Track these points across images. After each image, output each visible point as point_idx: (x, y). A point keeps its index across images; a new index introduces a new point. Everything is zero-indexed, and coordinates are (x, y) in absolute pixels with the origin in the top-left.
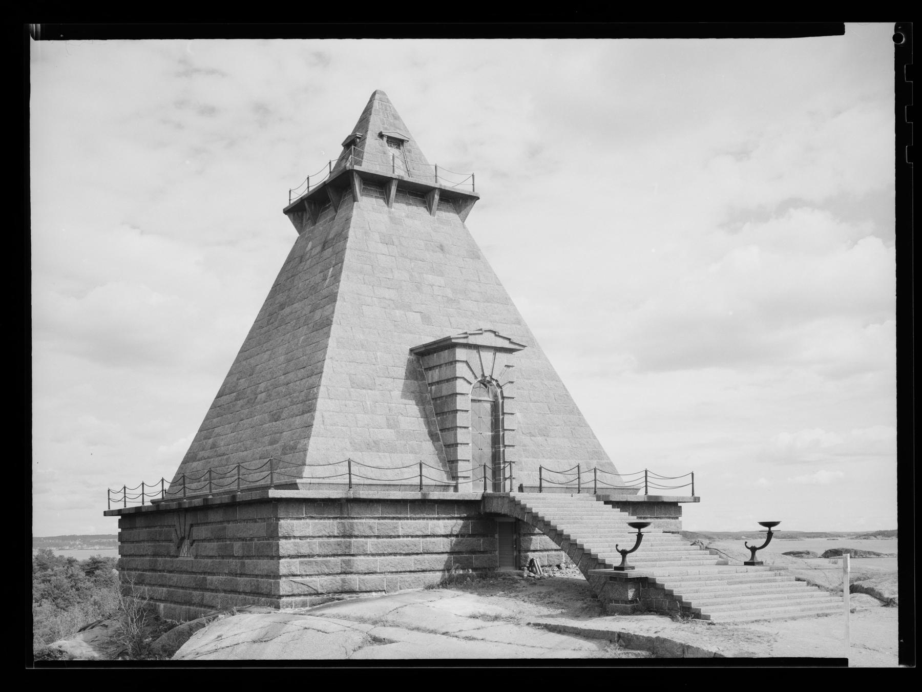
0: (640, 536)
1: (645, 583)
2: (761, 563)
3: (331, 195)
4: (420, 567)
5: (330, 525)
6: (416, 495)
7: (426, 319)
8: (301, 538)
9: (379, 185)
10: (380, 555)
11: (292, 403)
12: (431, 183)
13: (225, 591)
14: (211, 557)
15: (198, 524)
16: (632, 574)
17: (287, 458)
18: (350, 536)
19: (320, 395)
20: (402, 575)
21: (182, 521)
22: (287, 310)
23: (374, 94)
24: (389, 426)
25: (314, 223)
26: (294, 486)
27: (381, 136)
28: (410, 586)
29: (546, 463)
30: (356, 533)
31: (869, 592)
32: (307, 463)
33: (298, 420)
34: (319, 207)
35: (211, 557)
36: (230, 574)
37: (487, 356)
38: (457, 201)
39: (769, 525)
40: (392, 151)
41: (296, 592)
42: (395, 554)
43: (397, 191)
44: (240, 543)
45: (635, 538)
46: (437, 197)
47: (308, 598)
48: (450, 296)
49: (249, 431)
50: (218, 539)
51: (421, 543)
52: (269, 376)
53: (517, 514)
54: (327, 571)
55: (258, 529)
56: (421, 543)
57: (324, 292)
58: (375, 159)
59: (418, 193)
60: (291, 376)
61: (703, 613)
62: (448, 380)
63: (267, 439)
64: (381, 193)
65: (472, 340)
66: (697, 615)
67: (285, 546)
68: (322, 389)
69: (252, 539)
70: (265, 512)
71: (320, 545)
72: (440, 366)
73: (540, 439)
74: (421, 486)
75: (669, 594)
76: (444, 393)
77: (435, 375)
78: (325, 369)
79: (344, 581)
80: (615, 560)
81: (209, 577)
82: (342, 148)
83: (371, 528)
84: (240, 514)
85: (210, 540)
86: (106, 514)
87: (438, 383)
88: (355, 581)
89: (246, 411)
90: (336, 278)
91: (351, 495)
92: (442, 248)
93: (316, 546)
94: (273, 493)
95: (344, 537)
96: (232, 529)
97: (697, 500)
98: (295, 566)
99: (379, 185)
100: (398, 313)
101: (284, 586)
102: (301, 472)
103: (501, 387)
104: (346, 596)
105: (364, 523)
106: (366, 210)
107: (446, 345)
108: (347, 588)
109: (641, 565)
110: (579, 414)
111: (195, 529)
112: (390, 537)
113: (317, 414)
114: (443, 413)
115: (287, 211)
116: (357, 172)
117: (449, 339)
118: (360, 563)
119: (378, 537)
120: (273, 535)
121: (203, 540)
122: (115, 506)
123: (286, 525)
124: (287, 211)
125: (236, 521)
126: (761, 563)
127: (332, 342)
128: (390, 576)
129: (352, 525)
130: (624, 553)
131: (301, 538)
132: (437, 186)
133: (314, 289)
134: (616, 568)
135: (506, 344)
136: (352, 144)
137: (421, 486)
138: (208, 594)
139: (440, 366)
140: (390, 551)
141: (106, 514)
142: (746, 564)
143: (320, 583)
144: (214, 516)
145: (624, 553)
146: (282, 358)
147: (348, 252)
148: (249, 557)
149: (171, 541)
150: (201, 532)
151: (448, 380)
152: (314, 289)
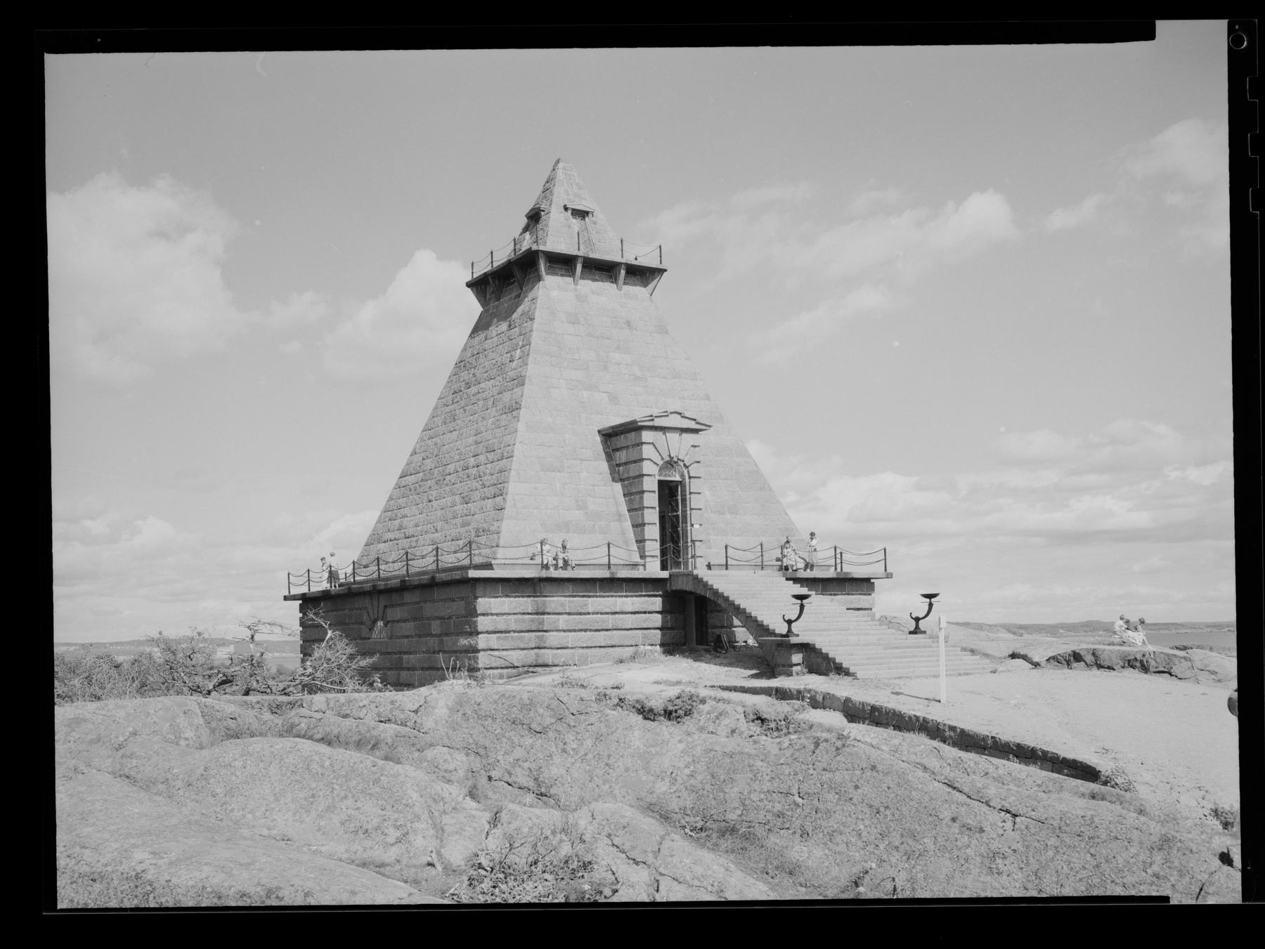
0: (802, 607)
1: (806, 648)
2: (925, 632)
3: (517, 273)
4: (609, 643)
5: (524, 603)
6: (605, 574)
7: (614, 399)
8: (497, 615)
9: (563, 263)
10: (570, 631)
11: (484, 486)
12: (618, 259)
13: (423, 669)
14: (407, 637)
15: (393, 606)
16: (794, 640)
17: (483, 540)
18: (543, 614)
19: (511, 479)
20: (593, 650)
21: (375, 603)
22: (473, 390)
23: (558, 161)
24: (579, 508)
25: (499, 299)
26: (489, 566)
27: (566, 209)
28: (600, 661)
29: (734, 541)
30: (548, 610)
31: (1024, 657)
32: (501, 543)
33: (489, 503)
34: (503, 284)
35: (407, 637)
36: (428, 652)
37: (673, 437)
38: (642, 274)
39: (930, 596)
40: (576, 223)
41: (494, 665)
42: (586, 630)
43: (584, 267)
44: (438, 622)
45: (798, 608)
46: (623, 272)
47: (505, 671)
48: (638, 373)
49: (439, 513)
50: (415, 619)
51: (610, 621)
52: (457, 457)
53: (700, 591)
54: (522, 646)
55: (457, 608)
56: (610, 621)
57: (512, 374)
58: (559, 236)
59: (603, 269)
60: (482, 458)
61: (851, 671)
62: (635, 462)
63: (459, 521)
64: (567, 270)
65: (658, 422)
66: (847, 673)
67: (483, 623)
68: (513, 473)
69: (450, 618)
70: (463, 591)
71: (516, 621)
72: (627, 447)
73: (728, 516)
74: (609, 565)
75: (826, 657)
76: (632, 474)
77: (622, 456)
78: (516, 453)
79: (537, 655)
80: (782, 628)
81: (405, 657)
82: (525, 220)
83: (562, 605)
84: (438, 593)
85: (405, 621)
86: (286, 598)
87: (625, 464)
88: (548, 656)
89: (434, 493)
90: (524, 357)
91: (544, 574)
92: (628, 323)
93: (512, 622)
94: (473, 574)
95: (537, 614)
96: (429, 609)
97: (889, 576)
98: (493, 641)
99: (563, 263)
100: (585, 394)
101: (483, 659)
102: (494, 553)
103: (687, 467)
104: (539, 669)
105: (555, 601)
106: (552, 289)
107: (632, 428)
108: (540, 662)
109: (804, 632)
110: (771, 489)
111: (389, 611)
112: (581, 614)
113: (509, 498)
114: (631, 494)
115: (469, 285)
116: (543, 252)
117: (635, 422)
118: (553, 638)
119: (569, 614)
120: (473, 613)
121: (398, 621)
122: (296, 591)
123: (483, 603)
124: (469, 285)
125: (433, 601)
126: (925, 632)
127: (521, 426)
128: (581, 651)
129: (544, 602)
130: (790, 622)
131: (497, 615)
132: (623, 261)
133: (501, 367)
134: (782, 636)
135: (693, 425)
136: (535, 217)
137: (609, 565)
138: (404, 674)
139: (627, 447)
140: (580, 627)
141: (286, 598)
142: (911, 633)
143: (516, 657)
144: (409, 597)
145: (790, 622)
146: (471, 440)
147: (534, 334)
148: (447, 635)
149: (362, 623)
150: (395, 613)
151: (635, 462)
152: (501, 367)
